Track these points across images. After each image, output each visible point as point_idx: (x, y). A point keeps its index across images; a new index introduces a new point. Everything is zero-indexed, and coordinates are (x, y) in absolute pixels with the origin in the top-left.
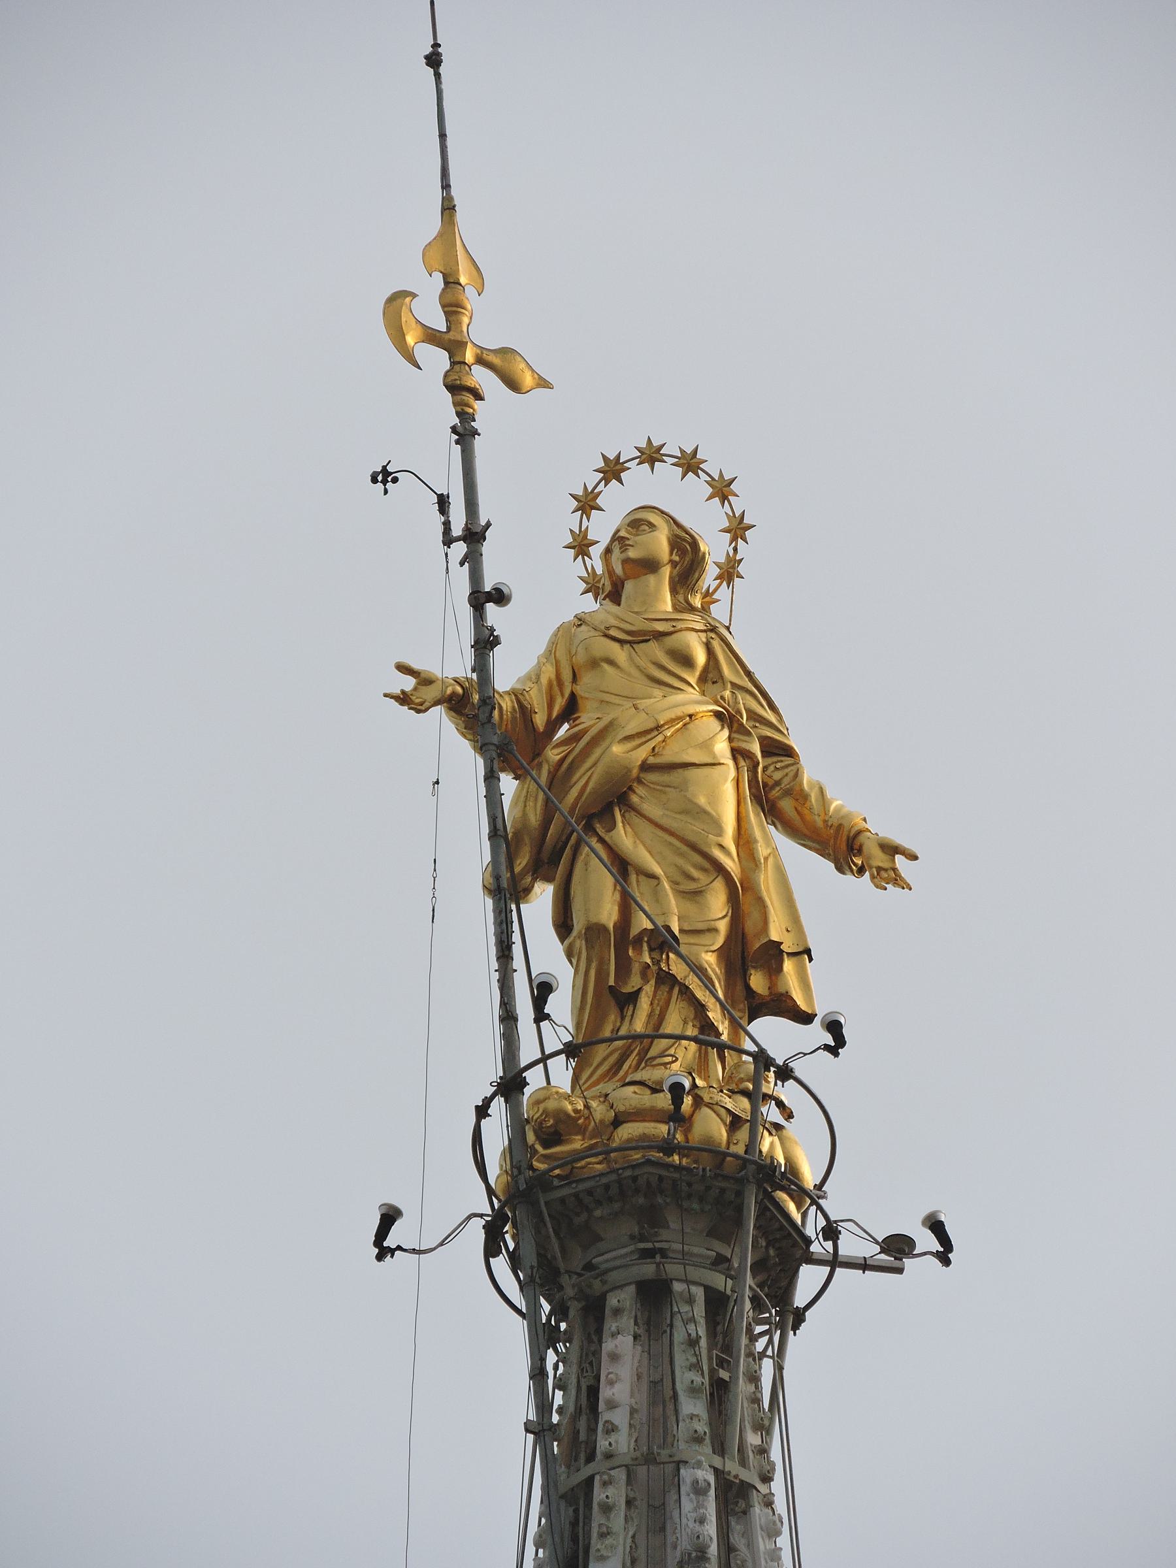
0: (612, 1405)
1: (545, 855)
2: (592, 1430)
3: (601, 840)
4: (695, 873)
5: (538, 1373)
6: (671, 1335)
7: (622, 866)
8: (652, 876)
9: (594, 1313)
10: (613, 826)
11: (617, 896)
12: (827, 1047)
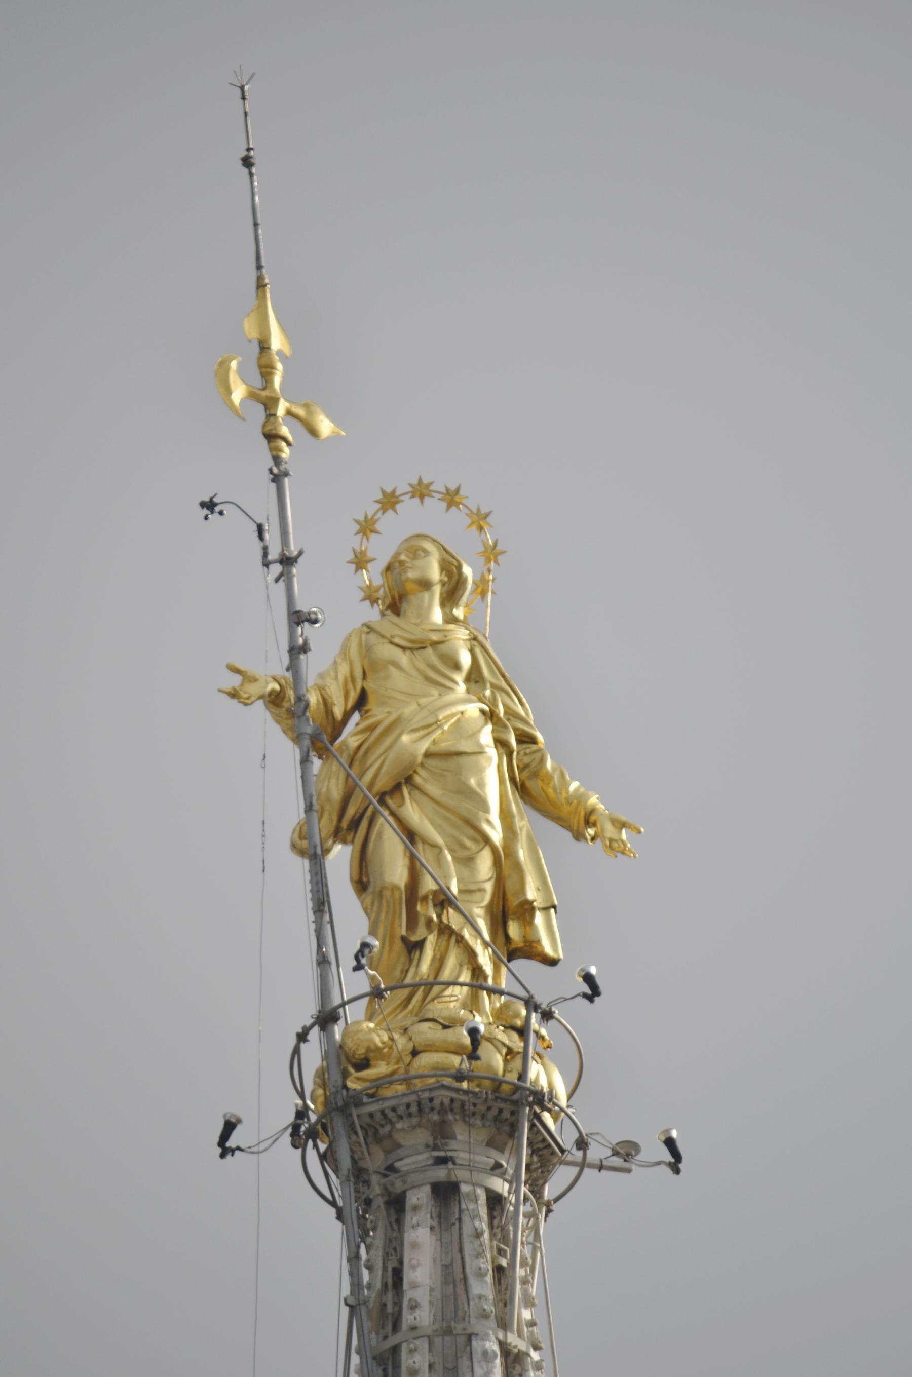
0: (414, 1286)
1: (345, 824)
2: (398, 1303)
3: (392, 814)
4: (468, 843)
5: (354, 1258)
6: (460, 1228)
7: (411, 835)
8: (435, 846)
9: (397, 1204)
10: (402, 803)
11: (406, 861)
12: (585, 996)
